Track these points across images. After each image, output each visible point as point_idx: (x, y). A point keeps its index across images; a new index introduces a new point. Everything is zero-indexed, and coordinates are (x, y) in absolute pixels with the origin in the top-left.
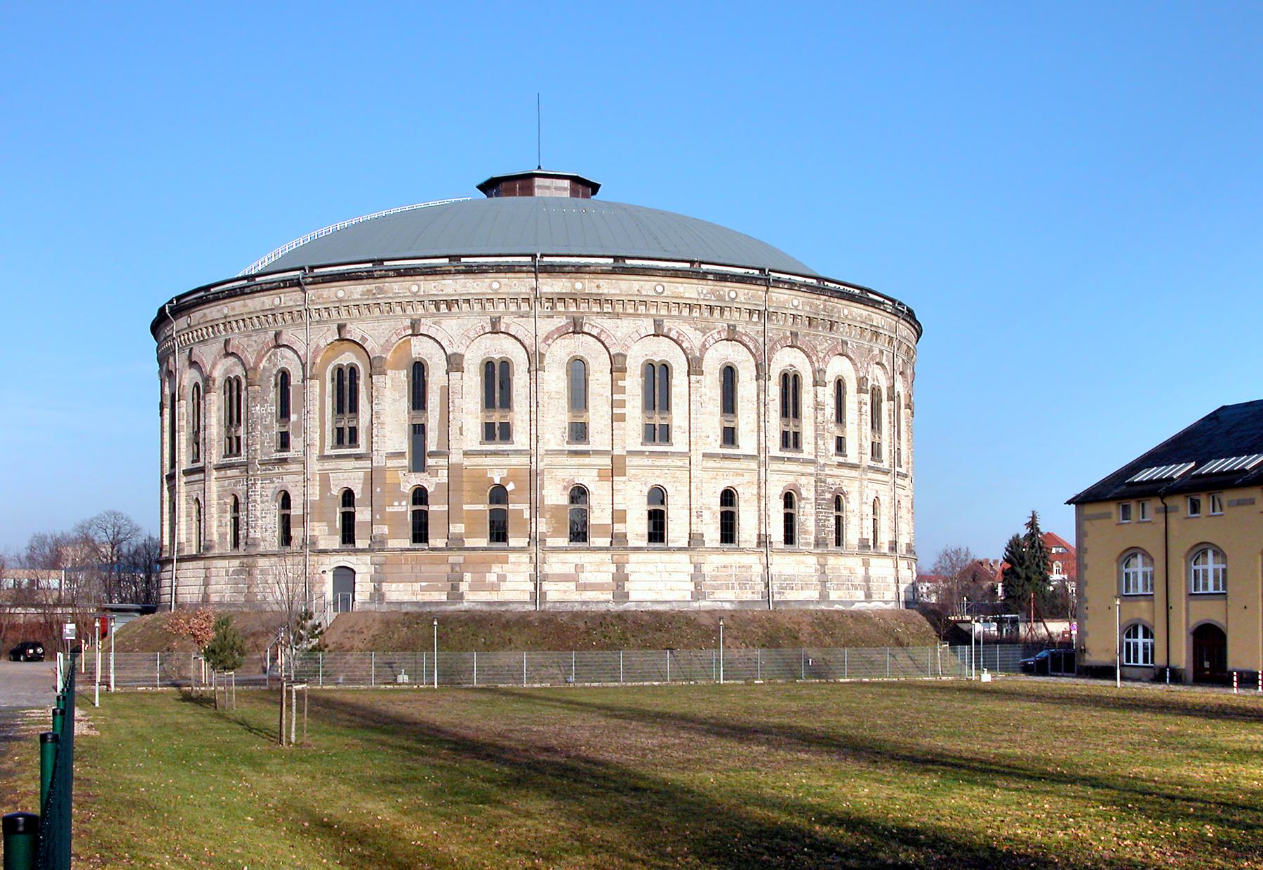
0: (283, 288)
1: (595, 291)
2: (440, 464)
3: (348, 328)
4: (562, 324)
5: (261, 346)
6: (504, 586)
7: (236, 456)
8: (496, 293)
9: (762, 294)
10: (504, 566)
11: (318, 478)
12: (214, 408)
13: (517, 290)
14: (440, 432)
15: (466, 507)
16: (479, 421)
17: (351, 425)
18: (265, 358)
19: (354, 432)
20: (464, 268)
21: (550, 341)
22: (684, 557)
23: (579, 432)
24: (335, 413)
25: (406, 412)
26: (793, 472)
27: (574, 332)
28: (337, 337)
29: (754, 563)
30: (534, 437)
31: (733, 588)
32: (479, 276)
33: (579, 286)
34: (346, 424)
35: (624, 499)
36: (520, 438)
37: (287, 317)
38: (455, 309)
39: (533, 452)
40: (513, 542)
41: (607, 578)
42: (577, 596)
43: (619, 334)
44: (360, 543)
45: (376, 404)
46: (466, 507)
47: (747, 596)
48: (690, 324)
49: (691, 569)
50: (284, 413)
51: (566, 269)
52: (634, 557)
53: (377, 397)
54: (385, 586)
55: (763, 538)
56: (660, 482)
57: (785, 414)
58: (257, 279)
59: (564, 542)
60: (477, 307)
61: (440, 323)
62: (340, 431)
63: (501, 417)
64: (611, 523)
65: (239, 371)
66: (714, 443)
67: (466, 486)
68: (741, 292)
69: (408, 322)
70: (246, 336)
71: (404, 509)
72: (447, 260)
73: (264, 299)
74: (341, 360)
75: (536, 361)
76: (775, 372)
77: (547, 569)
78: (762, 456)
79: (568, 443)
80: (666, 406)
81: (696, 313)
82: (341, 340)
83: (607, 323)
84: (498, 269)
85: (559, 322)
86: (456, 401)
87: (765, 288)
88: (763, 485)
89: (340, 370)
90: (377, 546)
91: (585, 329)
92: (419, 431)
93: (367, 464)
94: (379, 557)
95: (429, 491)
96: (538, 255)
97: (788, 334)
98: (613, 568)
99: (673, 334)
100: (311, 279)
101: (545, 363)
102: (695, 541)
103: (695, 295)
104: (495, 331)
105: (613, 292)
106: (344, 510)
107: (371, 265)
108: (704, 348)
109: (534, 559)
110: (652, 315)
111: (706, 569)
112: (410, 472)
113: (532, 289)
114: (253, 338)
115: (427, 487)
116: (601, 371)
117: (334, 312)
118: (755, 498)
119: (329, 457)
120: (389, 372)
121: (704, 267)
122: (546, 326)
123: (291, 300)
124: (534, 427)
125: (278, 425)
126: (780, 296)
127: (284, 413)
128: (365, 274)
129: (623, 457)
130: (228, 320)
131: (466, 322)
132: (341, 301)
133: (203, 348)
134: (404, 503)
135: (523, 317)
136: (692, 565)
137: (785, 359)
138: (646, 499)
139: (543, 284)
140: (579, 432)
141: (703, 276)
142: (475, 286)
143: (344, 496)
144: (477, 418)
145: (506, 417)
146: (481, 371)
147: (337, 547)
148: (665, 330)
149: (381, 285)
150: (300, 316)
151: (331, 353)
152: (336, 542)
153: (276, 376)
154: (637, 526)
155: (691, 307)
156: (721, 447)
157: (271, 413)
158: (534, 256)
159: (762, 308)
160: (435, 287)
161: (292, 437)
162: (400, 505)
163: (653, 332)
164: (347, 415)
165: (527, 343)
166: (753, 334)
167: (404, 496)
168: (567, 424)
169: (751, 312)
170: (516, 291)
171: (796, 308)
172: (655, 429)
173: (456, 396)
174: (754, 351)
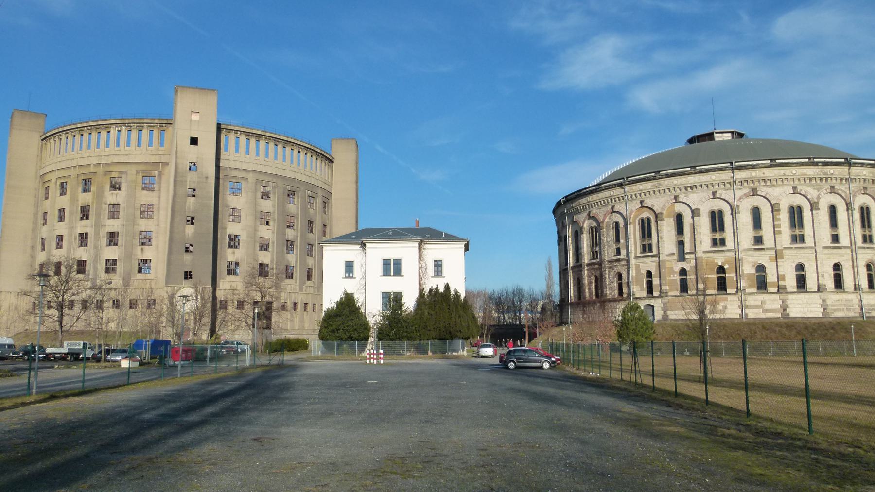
0: (615, 187)
1: (762, 175)
3: (645, 201)
4: (747, 192)
6: (727, 311)
7: (596, 259)
8: (714, 180)
9: (847, 170)
10: (726, 302)
11: (634, 266)
12: (585, 240)
13: (724, 178)
14: (691, 243)
16: (709, 238)
17: (649, 243)
19: (650, 246)
22: (817, 296)
23: (759, 240)
24: (641, 238)
26: (870, 254)
27: (752, 195)
28: (640, 206)
29: (854, 298)
30: (736, 243)
31: (844, 310)
32: (705, 174)
33: (754, 174)
35: (784, 270)
36: (730, 244)
37: (617, 199)
38: (695, 189)
39: (737, 250)
40: (729, 291)
41: (779, 307)
42: (763, 316)
44: (656, 294)
47: (851, 314)
48: (810, 187)
49: (821, 302)
50: (618, 240)
51: (748, 167)
52: (791, 296)
53: (660, 230)
54: (669, 313)
55: (857, 286)
56: (801, 261)
57: (863, 226)
58: (603, 185)
59: (755, 290)
60: (705, 187)
62: (644, 246)
63: (720, 235)
64: (777, 281)
65: (595, 224)
66: (827, 241)
68: (836, 170)
69: (673, 197)
71: (675, 278)
72: (689, 169)
75: (734, 210)
76: (856, 207)
77: (747, 303)
78: (853, 247)
79: (753, 245)
81: (813, 182)
82: (642, 207)
83: (768, 190)
84: (714, 170)
85: (746, 191)
87: (848, 167)
88: (855, 261)
89: (643, 220)
90: (663, 294)
91: (758, 193)
92: (681, 244)
93: (657, 259)
94: (665, 300)
96: (733, 162)
97: (862, 188)
98: (781, 302)
99: (803, 193)
101: (740, 209)
102: (820, 289)
103: (812, 173)
104: (714, 197)
105: (771, 175)
106: (647, 280)
107: (654, 174)
108: (818, 197)
109: (740, 299)
110: (791, 185)
111: (829, 302)
113: (731, 177)
114: (602, 209)
116: (767, 212)
117: (638, 195)
118: (851, 267)
119: (639, 257)
120: (665, 219)
121: (816, 160)
122: (739, 193)
126: (855, 170)
127: (618, 240)
129: (781, 251)
130: (590, 203)
131: (700, 194)
132: (641, 190)
133: (579, 216)
135: (727, 190)
136: (821, 301)
137: (861, 200)
138: (794, 269)
140: (759, 240)
141: (816, 164)
143: (647, 274)
146: (709, 216)
147: (645, 296)
148: (798, 191)
150: (623, 199)
151: (638, 213)
152: (644, 294)
153: (613, 224)
154: (791, 282)
155: (810, 179)
156: (831, 243)
158: (731, 163)
159: (847, 177)
161: (621, 250)
162: (674, 276)
163: (792, 192)
165: (730, 201)
166: (843, 189)
167: (675, 272)
169: (842, 179)
171: (865, 175)
172: (796, 237)
174: (845, 197)
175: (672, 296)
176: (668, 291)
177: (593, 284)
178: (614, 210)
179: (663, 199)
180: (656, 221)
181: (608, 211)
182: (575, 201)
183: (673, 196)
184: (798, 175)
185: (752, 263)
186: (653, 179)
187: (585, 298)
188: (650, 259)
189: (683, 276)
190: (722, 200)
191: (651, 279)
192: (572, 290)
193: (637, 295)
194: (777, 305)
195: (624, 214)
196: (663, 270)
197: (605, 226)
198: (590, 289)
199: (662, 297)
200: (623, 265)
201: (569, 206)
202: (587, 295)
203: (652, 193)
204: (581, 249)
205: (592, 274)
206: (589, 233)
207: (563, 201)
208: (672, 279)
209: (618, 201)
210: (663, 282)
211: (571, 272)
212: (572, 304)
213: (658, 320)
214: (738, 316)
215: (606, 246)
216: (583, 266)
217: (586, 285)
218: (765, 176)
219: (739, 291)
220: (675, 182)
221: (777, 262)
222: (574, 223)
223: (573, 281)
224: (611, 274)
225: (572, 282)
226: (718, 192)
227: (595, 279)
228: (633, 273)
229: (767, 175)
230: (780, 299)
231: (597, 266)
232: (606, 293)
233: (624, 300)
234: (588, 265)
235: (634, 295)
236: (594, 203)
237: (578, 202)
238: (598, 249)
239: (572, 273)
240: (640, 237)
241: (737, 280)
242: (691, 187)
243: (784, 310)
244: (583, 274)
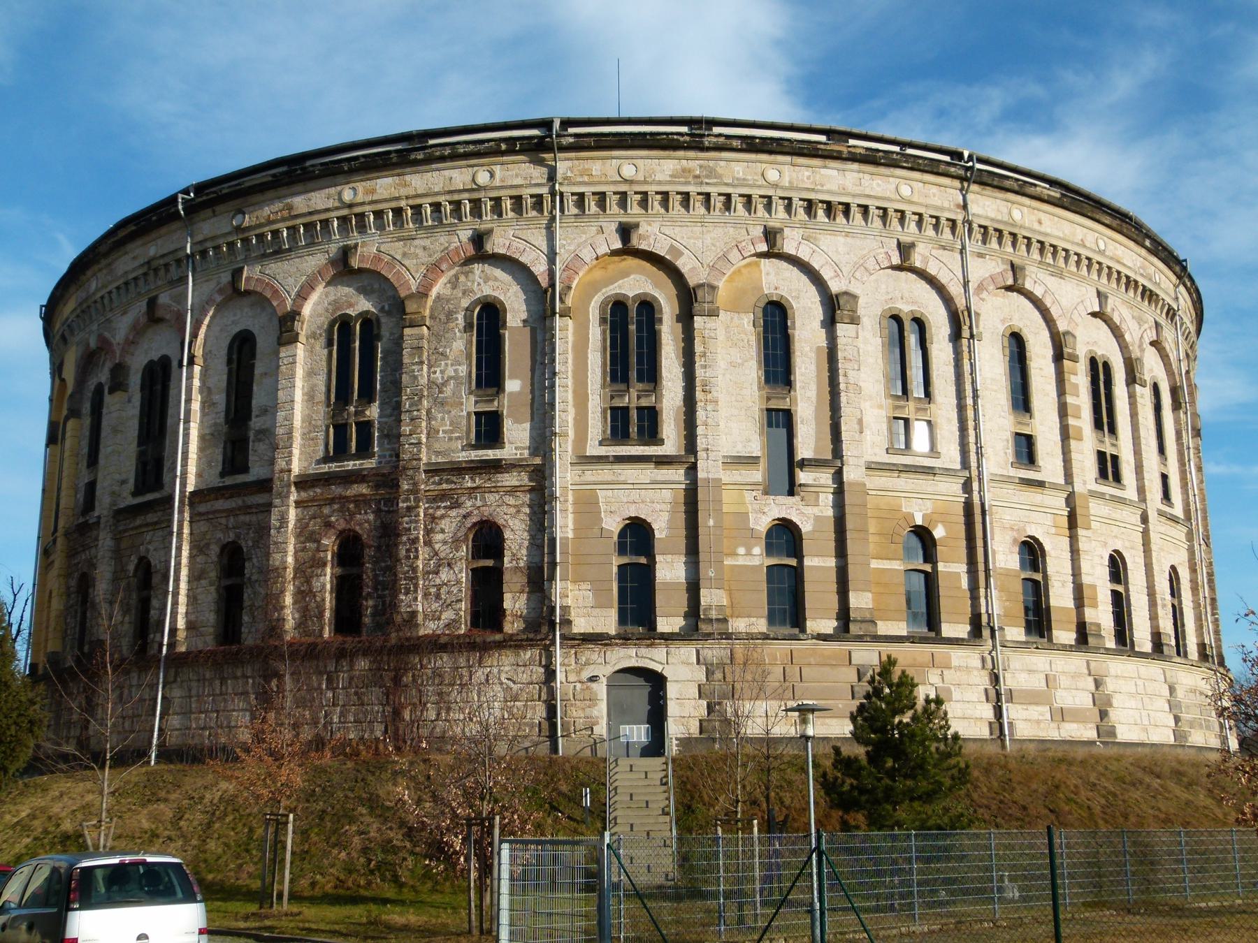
0: (503, 153)
1: (1036, 226)
2: (822, 482)
3: (641, 231)
4: (998, 270)
5: (437, 256)
11: (570, 498)
12: (300, 372)
15: (875, 564)
16: (884, 413)
17: (644, 402)
18: (443, 280)
20: (863, 152)
21: (984, 295)
23: (1026, 449)
25: (755, 387)
27: (1009, 289)
28: (618, 245)
34: (632, 399)
37: (507, 204)
39: (974, 473)
42: (1052, 732)
43: (1064, 302)
44: (668, 623)
45: (705, 367)
46: (875, 564)
53: (704, 355)
58: (431, 142)
60: (878, 223)
61: (815, 239)
65: (364, 305)
67: (872, 527)
69: (758, 231)
70: (399, 240)
72: (823, 138)
73: (455, 174)
74: (620, 287)
80: (1113, 430)
81: (1131, 293)
83: (1052, 282)
86: (851, 373)
91: (1028, 285)
93: (677, 474)
94: (715, 651)
95: (803, 530)
96: (966, 154)
99: (1117, 320)
100: (571, 140)
109: (989, 665)
112: (766, 493)
113: (958, 206)
114: (416, 242)
115: (798, 523)
116: (1044, 357)
117: (612, 201)
120: (722, 313)
123: (517, 176)
124: (971, 432)
125: (473, 399)
128: (687, 138)
130: (358, 210)
133: (277, 268)
134: (757, 550)
139: (972, 202)
140: (1026, 449)
142: (875, 185)
143: (622, 534)
144: (880, 407)
145: (926, 410)
149: (711, 163)
151: (598, 274)
152: (608, 622)
154: (1101, 615)
157: (455, 378)
160: (808, 178)
161: (508, 424)
162: (749, 553)
164: (636, 387)
168: (1008, 436)
170: (939, 203)
173: (848, 365)
175: (751, 637)
176: (728, 612)
177: (328, 570)
178: (489, 248)
179: (719, 231)
180: (686, 317)
181: (447, 255)
182: (260, 205)
183: (760, 229)
184: (1111, 258)
185: (1012, 529)
186: (689, 147)
187: (275, 628)
188: (647, 473)
189: (779, 554)
190: (923, 283)
191: (643, 560)
192: (182, 599)
193: (580, 625)
194: (1081, 699)
195: (540, 268)
196: (707, 522)
197: (427, 313)
198: (304, 595)
199: (708, 636)
200: (513, 491)
201: (213, 226)
202: (290, 617)
203: (675, 201)
204: (271, 410)
205: (328, 525)
206: (329, 344)
207: (185, 202)
208: (741, 561)
209: (511, 214)
210: (708, 572)
211: (187, 515)
212: (178, 662)
213: (685, 742)
214: (984, 732)
215: (425, 403)
216: (277, 485)
217: (290, 573)
218: (1042, 229)
219: (986, 633)
220: (772, 175)
221: (1073, 538)
222: (235, 293)
223: (192, 557)
224: (444, 524)
225: (185, 560)
226: (917, 249)
227: (340, 547)
228: (565, 524)
229: (1048, 231)
230: (1090, 675)
231: (364, 489)
232: (414, 614)
233: (514, 643)
234: (303, 483)
235: (567, 622)
236: (379, 214)
237: (278, 206)
238: (373, 412)
239: (191, 522)
240: (604, 372)
241: (974, 588)
242: (829, 207)
243: (1103, 714)
244: (274, 522)
